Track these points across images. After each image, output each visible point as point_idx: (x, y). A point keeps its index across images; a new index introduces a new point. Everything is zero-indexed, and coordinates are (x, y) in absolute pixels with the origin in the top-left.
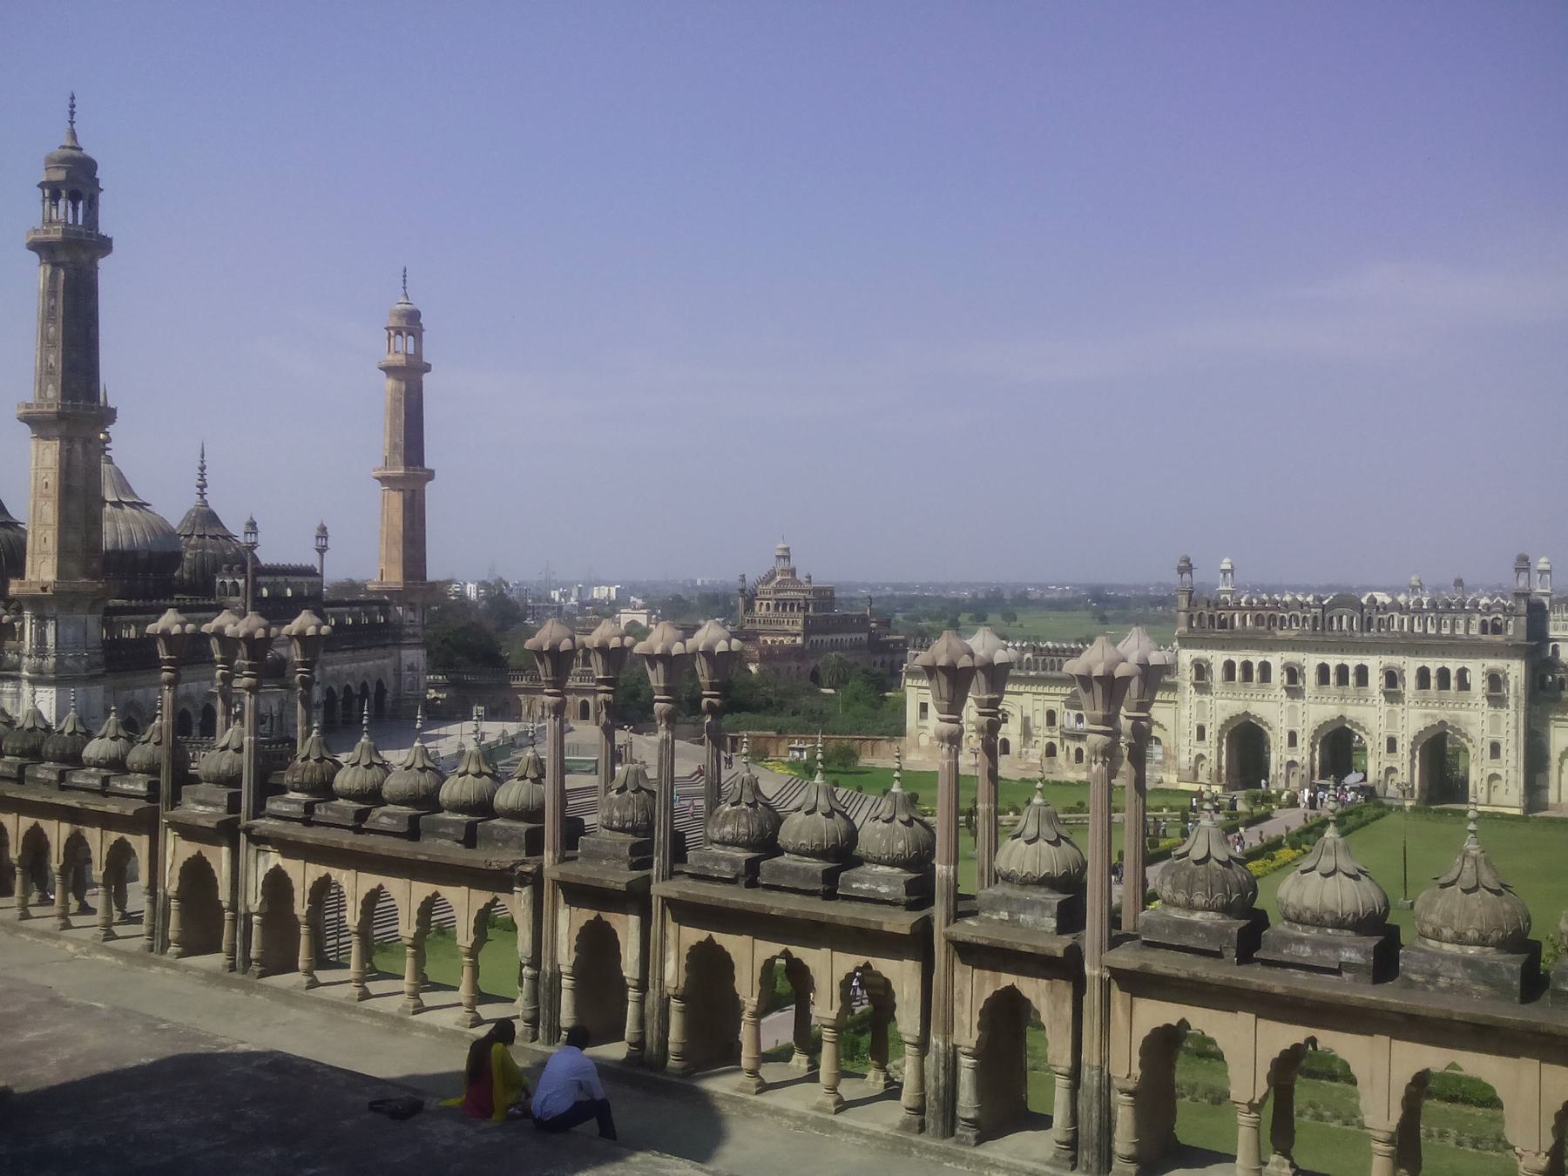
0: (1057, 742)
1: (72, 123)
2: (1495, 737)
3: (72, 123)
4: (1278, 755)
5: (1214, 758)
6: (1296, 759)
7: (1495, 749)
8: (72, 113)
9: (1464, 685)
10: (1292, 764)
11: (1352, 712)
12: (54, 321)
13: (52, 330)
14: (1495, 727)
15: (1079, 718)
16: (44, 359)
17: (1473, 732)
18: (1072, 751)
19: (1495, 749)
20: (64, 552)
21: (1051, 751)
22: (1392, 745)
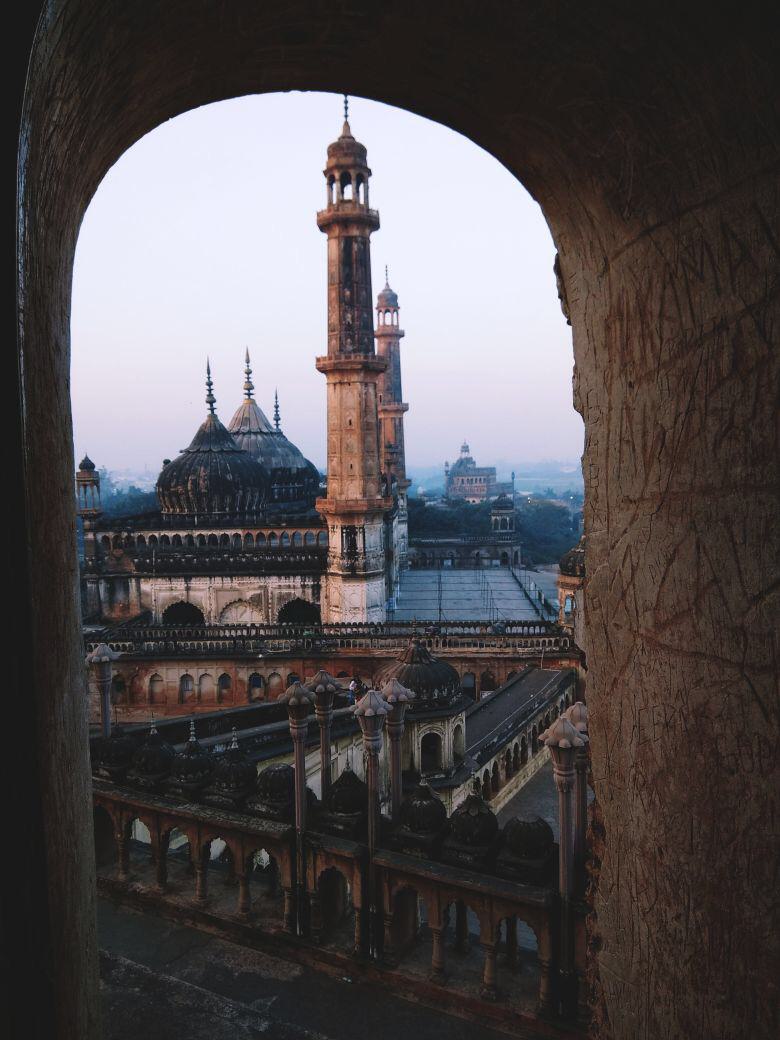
1: (346, 116)
3: (346, 116)
8: (346, 108)
12: (351, 288)
13: (348, 293)
16: (342, 318)
20: (366, 474)
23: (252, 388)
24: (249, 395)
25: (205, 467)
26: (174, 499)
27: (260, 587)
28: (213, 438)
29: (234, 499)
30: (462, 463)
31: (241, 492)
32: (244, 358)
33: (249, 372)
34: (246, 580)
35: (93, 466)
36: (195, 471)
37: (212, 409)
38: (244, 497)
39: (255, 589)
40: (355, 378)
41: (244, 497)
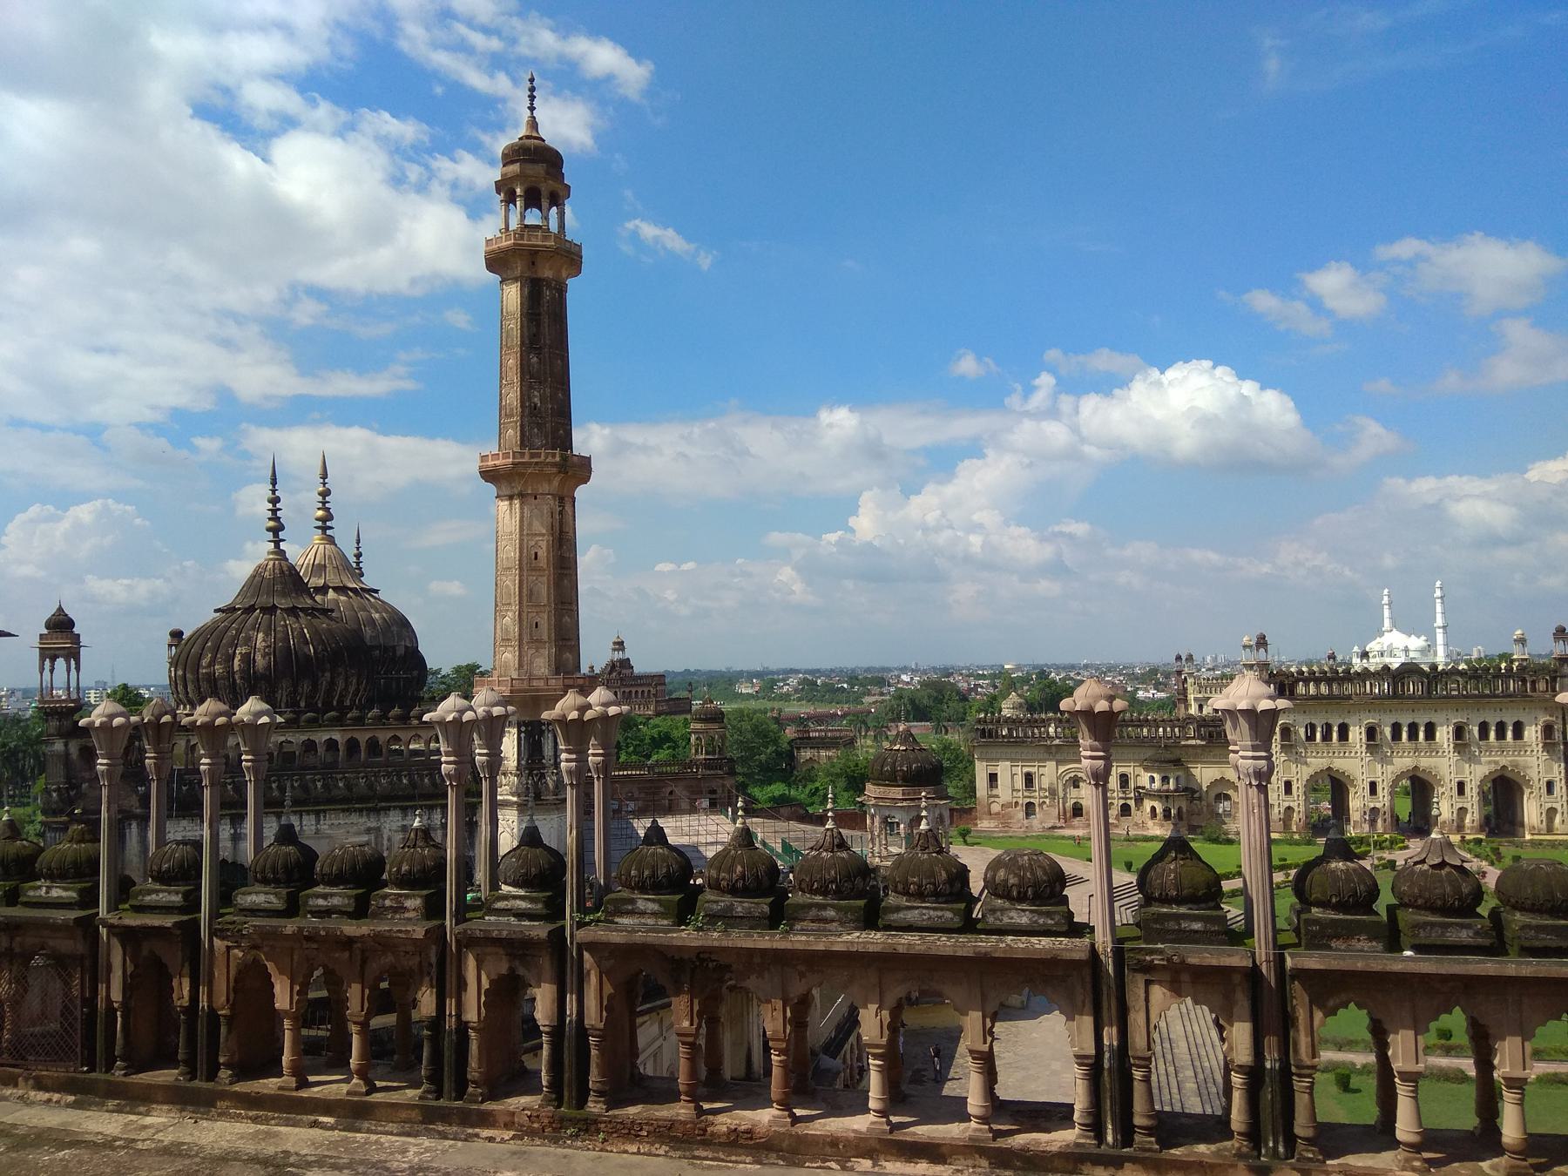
0: (1132, 803)
2: (1549, 777)
4: (1357, 803)
5: (1302, 809)
6: (1378, 805)
7: (1550, 785)
9: (1518, 735)
10: (1374, 811)
11: (1425, 762)
14: (1549, 770)
15: (1165, 780)
16: (525, 398)
17: (1533, 774)
18: (1159, 810)
19: (1550, 785)
21: (1125, 810)
22: (1461, 787)
23: (329, 517)
24: (324, 529)
25: (267, 634)
26: (204, 686)
27: (368, 831)
28: (278, 587)
29: (315, 686)
30: (613, 666)
31: (328, 674)
32: (319, 471)
33: (325, 494)
34: (342, 819)
35: (71, 624)
36: (248, 640)
37: (277, 543)
38: (332, 683)
39: (358, 834)
40: (545, 488)
41: (332, 683)
